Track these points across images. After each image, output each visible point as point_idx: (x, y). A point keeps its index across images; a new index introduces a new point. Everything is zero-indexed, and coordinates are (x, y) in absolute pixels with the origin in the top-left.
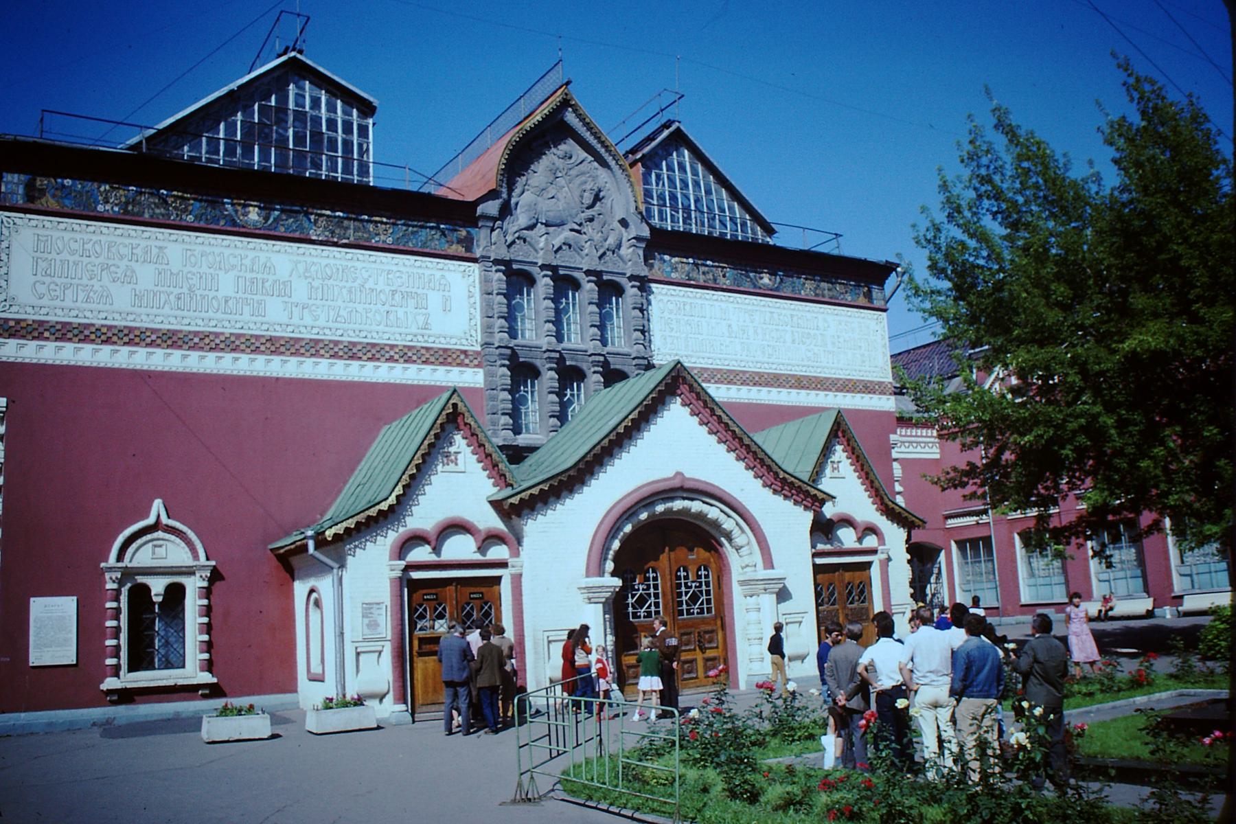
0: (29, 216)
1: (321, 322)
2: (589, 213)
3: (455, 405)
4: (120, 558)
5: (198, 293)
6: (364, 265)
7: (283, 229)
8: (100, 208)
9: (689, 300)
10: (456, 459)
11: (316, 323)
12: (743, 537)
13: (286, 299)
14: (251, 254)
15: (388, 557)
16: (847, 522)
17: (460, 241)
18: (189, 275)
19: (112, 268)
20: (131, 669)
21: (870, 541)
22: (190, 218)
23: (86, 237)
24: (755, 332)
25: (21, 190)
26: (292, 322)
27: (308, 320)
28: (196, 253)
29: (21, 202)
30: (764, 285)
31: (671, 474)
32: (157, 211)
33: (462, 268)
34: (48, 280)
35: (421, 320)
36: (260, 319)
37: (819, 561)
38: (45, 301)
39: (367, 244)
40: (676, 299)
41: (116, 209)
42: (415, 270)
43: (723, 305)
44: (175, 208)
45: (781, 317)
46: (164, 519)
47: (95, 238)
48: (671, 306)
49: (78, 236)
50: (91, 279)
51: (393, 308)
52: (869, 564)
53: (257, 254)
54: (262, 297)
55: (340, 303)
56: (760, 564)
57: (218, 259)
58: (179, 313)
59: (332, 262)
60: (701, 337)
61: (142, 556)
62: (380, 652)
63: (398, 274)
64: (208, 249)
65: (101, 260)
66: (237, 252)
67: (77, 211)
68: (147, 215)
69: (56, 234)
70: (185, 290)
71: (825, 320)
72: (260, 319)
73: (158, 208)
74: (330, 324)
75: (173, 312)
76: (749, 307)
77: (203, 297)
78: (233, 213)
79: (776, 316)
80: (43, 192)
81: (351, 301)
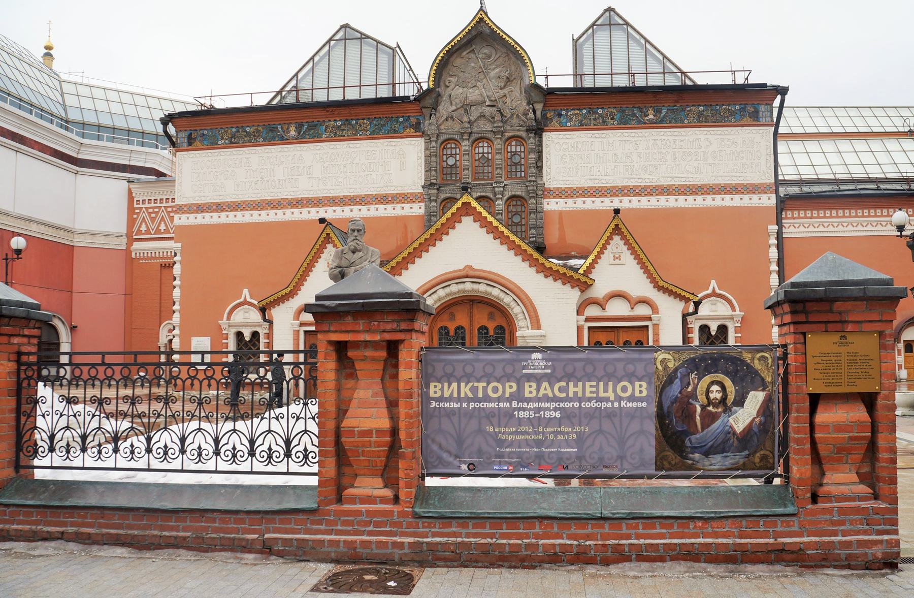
0: (189, 152)
2: (502, 92)
3: (328, 234)
4: (229, 318)
5: (266, 179)
8: (220, 142)
9: (581, 140)
13: (310, 176)
15: (292, 319)
17: (411, 126)
18: (261, 171)
19: (226, 173)
22: (261, 140)
25: (186, 141)
28: (264, 158)
30: (649, 120)
31: (462, 267)
32: (246, 139)
33: (413, 142)
39: (356, 137)
40: (571, 140)
41: (227, 142)
42: (384, 148)
43: (611, 140)
44: (254, 136)
45: (664, 143)
46: (248, 299)
47: (218, 158)
52: (647, 327)
57: (275, 159)
60: (589, 165)
61: (239, 317)
68: (241, 142)
73: (246, 137)
76: (634, 139)
78: (282, 133)
79: (658, 142)
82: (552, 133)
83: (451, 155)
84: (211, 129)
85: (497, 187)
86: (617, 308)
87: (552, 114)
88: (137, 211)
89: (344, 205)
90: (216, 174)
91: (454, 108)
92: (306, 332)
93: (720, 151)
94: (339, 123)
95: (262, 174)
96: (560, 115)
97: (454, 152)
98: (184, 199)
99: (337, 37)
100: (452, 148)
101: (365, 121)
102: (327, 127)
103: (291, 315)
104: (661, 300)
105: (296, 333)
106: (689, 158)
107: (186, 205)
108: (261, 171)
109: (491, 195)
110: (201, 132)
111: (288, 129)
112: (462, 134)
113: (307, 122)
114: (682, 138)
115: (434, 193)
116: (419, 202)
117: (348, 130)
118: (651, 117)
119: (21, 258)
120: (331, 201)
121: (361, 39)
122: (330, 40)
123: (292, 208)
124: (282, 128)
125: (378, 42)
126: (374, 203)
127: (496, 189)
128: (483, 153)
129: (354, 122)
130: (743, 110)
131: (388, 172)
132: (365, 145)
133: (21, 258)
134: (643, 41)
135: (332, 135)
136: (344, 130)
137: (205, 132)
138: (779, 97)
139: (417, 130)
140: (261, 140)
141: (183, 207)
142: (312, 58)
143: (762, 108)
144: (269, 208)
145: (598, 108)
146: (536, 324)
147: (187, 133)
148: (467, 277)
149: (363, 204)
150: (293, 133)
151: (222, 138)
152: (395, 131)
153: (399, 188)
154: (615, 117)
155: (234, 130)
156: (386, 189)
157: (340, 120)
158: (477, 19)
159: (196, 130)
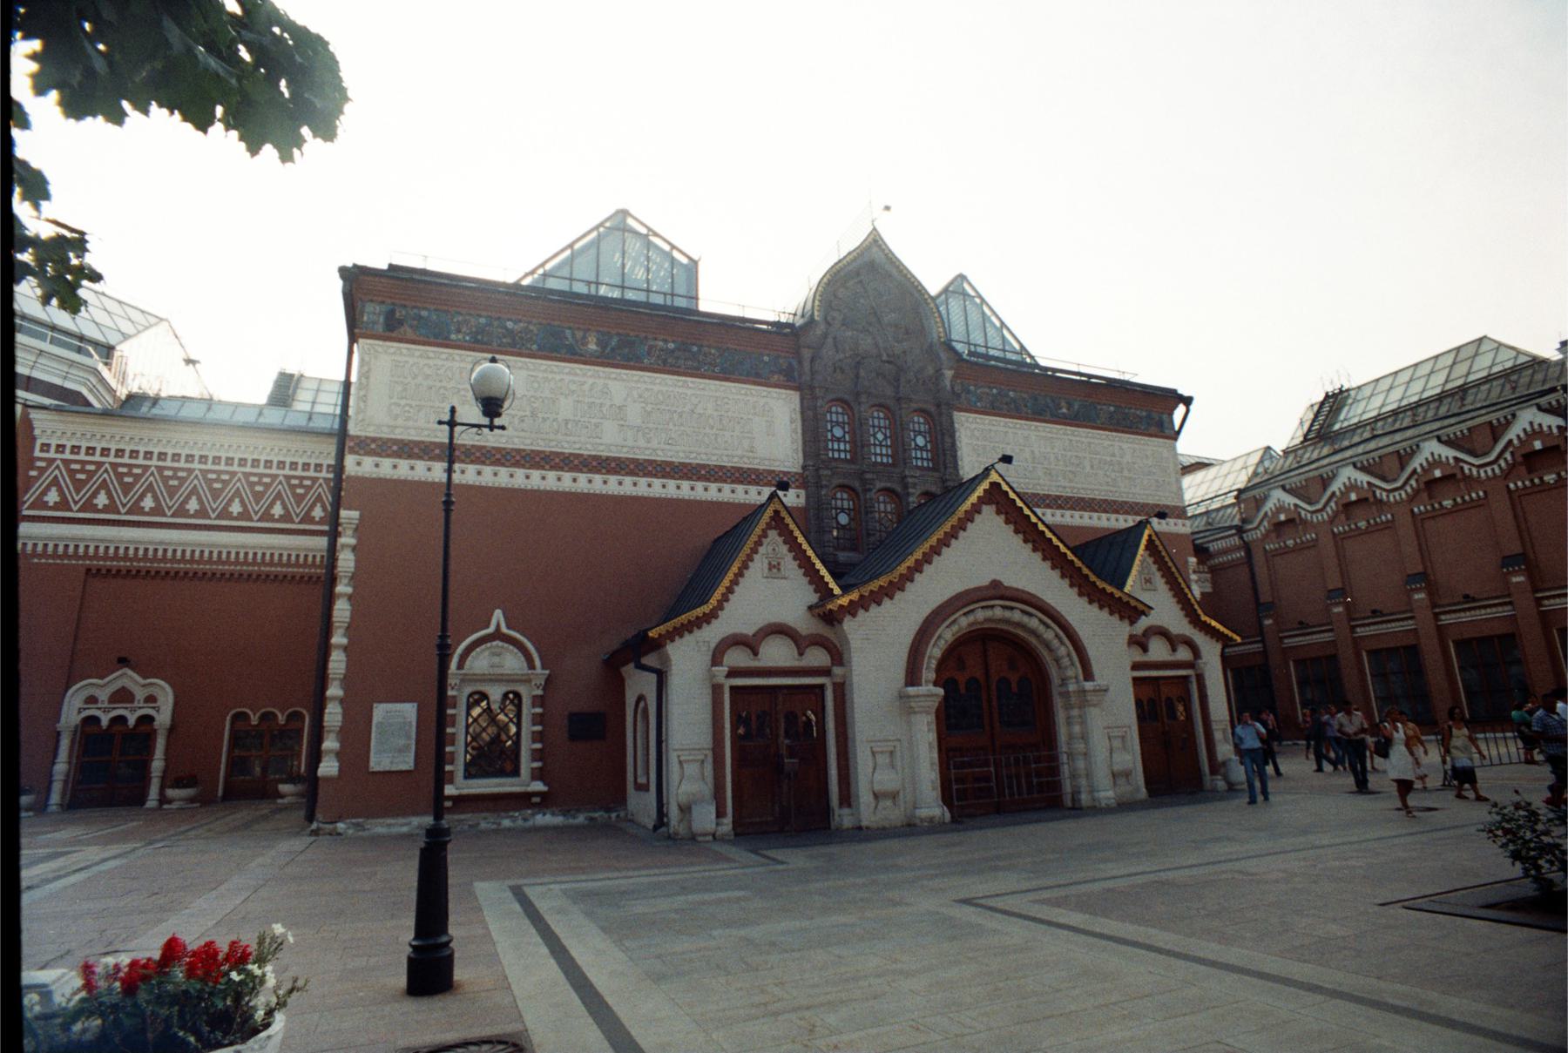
1: (654, 444)
5: (540, 415)
6: (693, 392)
7: (619, 358)
8: (453, 337)
10: (779, 564)
11: (649, 445)
12: (1064, 650)
13: (622, 422)
14: (590, 381)
16: (1163, 633)
18: (533, 399)
19: (462, 393)
21: (1184, 654)
23: (440, 363)
24: (1056, 458)
26: (625, 443)
27: (642, 443)
29: (381, 330)
30: (1063, 414)
31: (985, 582)
32: (504, 340)
34: (403, 402)
35: (746, 444)
36: (598, 441)
38: (400, 422)
41: (467, 338)
43: (1026, 433)
47: (448, 364)
48: (976, 433)
49: (431, 362)
50: (443, 402)
51: (721, 433)
53: (597, 381)
54: (599, 421)
55: (671, 426)
58: (522, 434)
59: (664, 389)
62: (703, 762)
63: (726, 400)
64: (550, 376)
65: (452, 384)
66: (576, 379)
67: (432, 340)
68: (495, 344)
69: (411, 361)
70: (528, 413)
71: (1121, 448)
72: (598, 441)
73: (505, 337)
74: (663, 446)
75: (516, 434)
77: (544, 420)
78: (574, 343)
80: (401, 323)
81: (682, 425)
82: (962, 414)
83: (838, 423)
84: (436, 310)
85: (912, 476)
86: (1158, 650)
87: (960, 387)
88: (39, 464)
89: (681, 478)
90: (442, 391)
91: (842, 356)
92: (732, 688)
93: (1134, 463)
94: (671, 346)
95: (535, 405)
96: (969, 392)
97: (841, 420)
98: (371, 429)
99: (608, 224)
100: (837, 413)
101: (713, 351)
102: (651, 347)
103: (708, 658)
104: (1200, 638)
105: (716, 689)
106: (1106, 468)
107: (374, 440)
108: (533, 399)
109: (899, 489)
110: (415, 311)
111: (584, 337)
112: (858, 394)
113: (618, 334)
114: (1096, 441)
115: (826, 476)
116: (797, 487)
117: (685, 359)
118: (1064, 410)
119: (503, 428)
120: (659, 469)
121: (647, 235)
122: (601, 225)
123: (590, 471)
124: (573, 335)
125: (673, 247)
126: (729, 481)
127: (910, 480)
128: (880, 427)
129: (695, 349)
130: (1149, 417)
131: (749, 435)
132: (713, 387)
133: (503, 428)
134: (998, 324)
135: (660, 362)
136: (678, 358)
137: (424, 313)
138: (1181, 409)
139: (789, 379)
140: (535, 347)
141: (368, 441)
142: (571, 246)
143: (1165, 417)
144: (547, 467)
145: (1009, 390)
146: (1088, 675)
147: (384, 308)
148: (1002, 598)
149: (712, 479)
150: (592, 347)
151: (459, 331)
152: (758, 375)
153: (767, 463)
154: (1029, 404)
155: (483, 320)
156: (746, 460)
157: (673, 342)
158: (870, 240)
159: (405, 306)
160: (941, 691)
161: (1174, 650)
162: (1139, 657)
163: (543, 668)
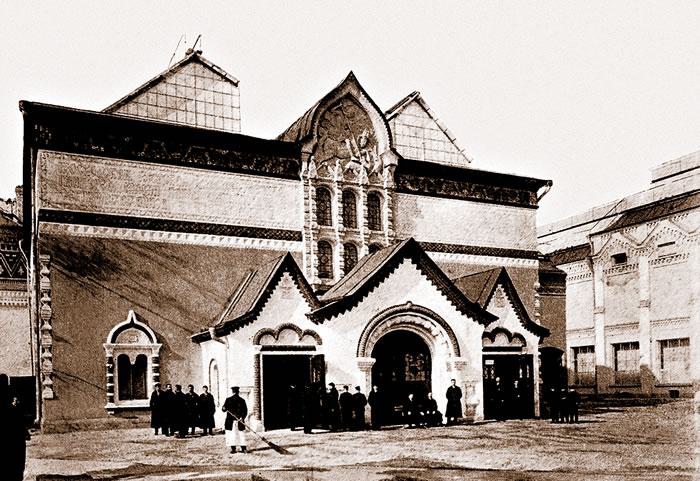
20: (120, 399)
21: (517, 343)
37: (486, 353)
46: (135, 321)
56: (453, 354)
86: (501, 341)
92: (264, 356)
105: (258, 356)
160: (374, 360)
161: (510, 341)
162: (489, 344)
163: (158, 342)
